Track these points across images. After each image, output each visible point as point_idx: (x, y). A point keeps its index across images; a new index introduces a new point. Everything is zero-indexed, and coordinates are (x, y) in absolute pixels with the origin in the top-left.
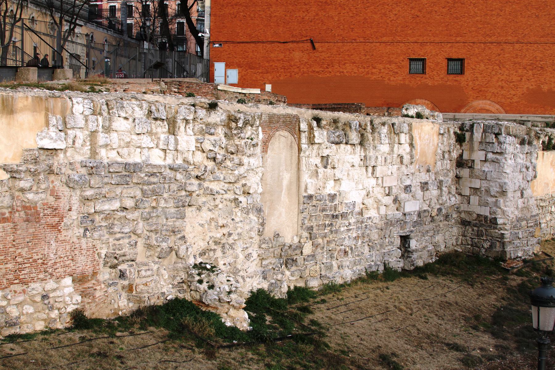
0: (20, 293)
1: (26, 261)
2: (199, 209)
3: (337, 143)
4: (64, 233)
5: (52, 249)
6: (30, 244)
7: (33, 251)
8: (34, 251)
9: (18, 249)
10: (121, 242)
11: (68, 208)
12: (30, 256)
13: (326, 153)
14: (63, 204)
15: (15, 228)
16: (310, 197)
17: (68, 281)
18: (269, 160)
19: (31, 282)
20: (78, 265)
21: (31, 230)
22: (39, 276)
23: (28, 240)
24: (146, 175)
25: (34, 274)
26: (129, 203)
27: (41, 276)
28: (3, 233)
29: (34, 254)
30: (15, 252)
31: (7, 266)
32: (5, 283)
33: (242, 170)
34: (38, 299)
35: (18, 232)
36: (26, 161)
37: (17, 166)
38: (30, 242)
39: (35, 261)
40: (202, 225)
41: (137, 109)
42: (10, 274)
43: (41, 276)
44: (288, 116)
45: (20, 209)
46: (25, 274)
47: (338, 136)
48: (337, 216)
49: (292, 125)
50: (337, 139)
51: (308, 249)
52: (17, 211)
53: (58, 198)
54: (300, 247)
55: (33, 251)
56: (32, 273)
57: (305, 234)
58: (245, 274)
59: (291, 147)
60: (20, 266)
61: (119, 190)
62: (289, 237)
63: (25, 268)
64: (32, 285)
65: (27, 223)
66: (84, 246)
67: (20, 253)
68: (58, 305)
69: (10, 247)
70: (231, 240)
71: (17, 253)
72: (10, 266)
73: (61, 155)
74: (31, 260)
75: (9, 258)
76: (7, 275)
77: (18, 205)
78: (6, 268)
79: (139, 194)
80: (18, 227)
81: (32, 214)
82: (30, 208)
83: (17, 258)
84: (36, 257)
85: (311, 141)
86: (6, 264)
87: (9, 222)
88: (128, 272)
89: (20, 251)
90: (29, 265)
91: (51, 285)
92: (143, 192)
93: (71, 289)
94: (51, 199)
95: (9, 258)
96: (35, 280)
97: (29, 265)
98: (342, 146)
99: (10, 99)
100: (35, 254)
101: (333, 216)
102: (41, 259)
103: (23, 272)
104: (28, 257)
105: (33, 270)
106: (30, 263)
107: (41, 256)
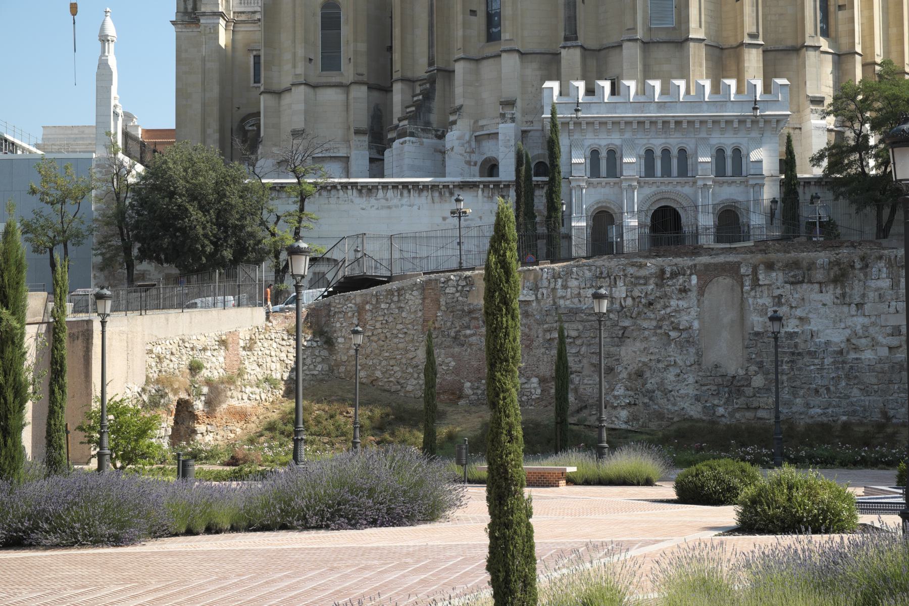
2: (635, 339)
3: (792, 283)
4: (534, 351)
13: (777, 292)
14: (533, 333)
16: (757, 334)
17: (535, 380)
18: (706, 302)
33: (668, 310)
40: (634, 352)
41: (587, 272)
44: (728, 263)
47: (794, 276)
48: (799, 354)
49: (732, 270)
50: (793, 280)
51: (758, 381)
54: (748, 379)
57: (753, 368)
58: (676, 394)
59: (732, 290)
62: (733, 367)
70: (660, 365)
73: (534, 304)
79: (581, 327)
85: (756, 283)
92: (584, 327)
98: (805, 286)
101: (793, 354)
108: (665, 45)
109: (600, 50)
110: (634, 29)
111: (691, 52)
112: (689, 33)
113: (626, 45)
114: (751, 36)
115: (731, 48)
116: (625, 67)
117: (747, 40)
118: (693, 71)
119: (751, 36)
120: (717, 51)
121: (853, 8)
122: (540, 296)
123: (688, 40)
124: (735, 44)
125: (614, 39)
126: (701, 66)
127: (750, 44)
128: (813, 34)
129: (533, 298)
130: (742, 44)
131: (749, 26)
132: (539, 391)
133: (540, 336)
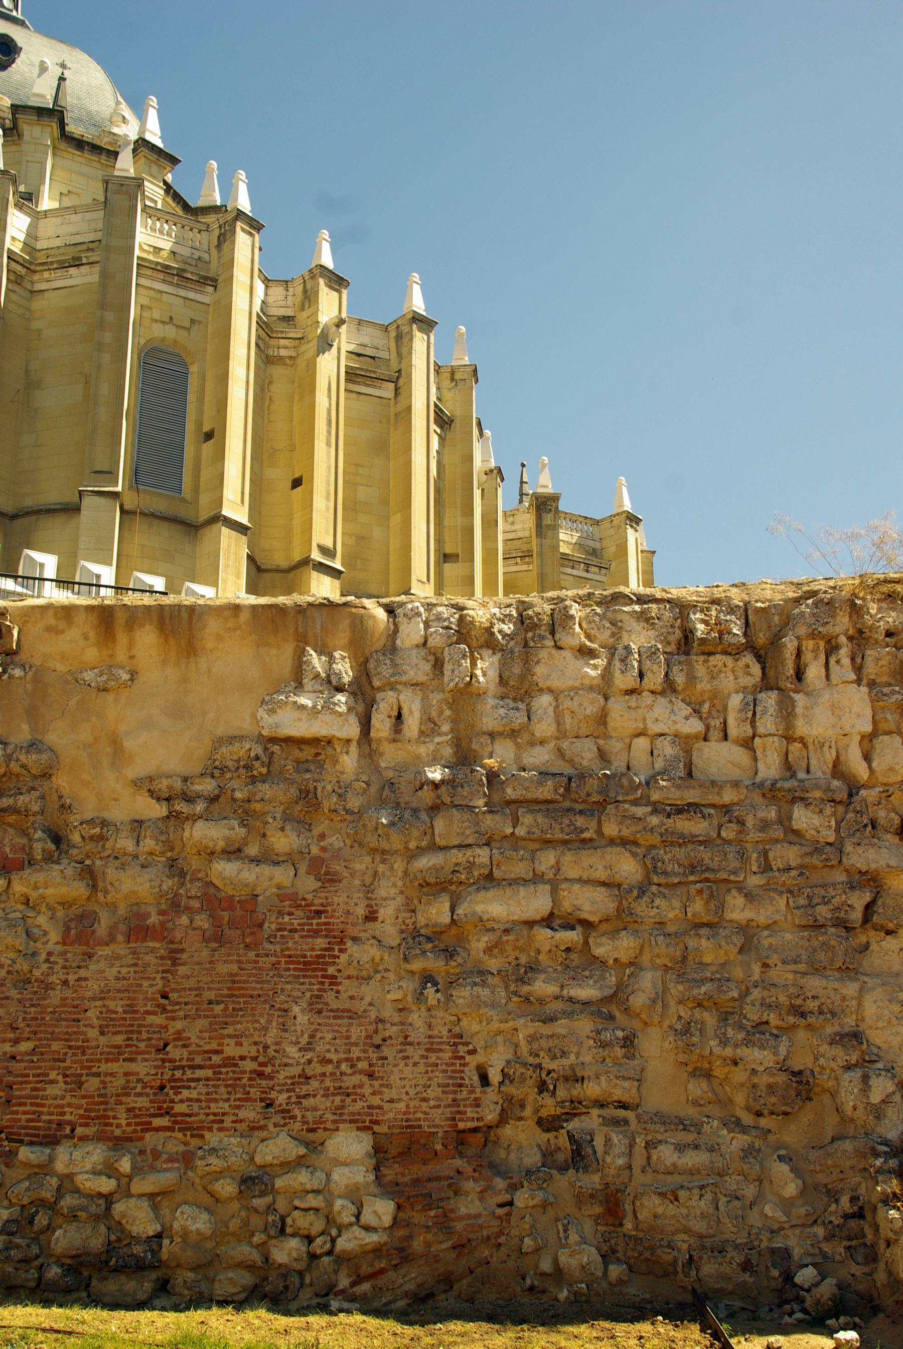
0: (171, 1160)
1: (198, 1060)
4: (347, 988)
5: (294, 1034)
6: (218, 1009)
7: (225, 1032)
8: (230, 1030)
9: (173, 1019)
10: (560, 1027)
11: (361, 911)
12: (214, 1046)
14: (347, 901)
15: (174, 957)
17: (350, 1147)
19: (210, 1129)
20: (388, 1094)
21: (223, 969)
22: (242, 1114)
23: (212, 995)
24: (655, 811)
25: (221, 1104)
26: (591, 902)
27: (249, 1113)
28: (132, 969)
29: (226, 1041)
30: (166, 1027)
31: (132, 1067)
32: (123, 1122)
34: (227, 1188)
35: (182, 970)
36: (215, 770)
37: (185, 780)
38: (218, 1003)
39: (230, 1062)
42: (139, 1095)
43: (249, 1113)
45: (196, 904)
46: (189, 1100)
52: (187, 908)
53: (329, 879)
55: (225, 1032)
56: (216, 1100)
60: (178, 1074)
61: (547, 860)
63: (198, 1080)
64: (213, 1138)
65: (214, 945)
66: (419, 1032)
67: (179, 1032)
68: (300, 1220)
69: (148, 1013)
71: (171, 1031)
72: (142, 1068)
74: (216, 1059)
75: (142, 1045)
76: (128, 1095)
77: (193, 893)
78: (126, 1074)
80: (185, 956)
81: (236, 919)
82: (229, 903)
83: (168, 1048)
84: (231, 1050)
86: (131, 1060)
87: (155, 939)
88: (599, 1142)
89: (179, 1025)
90: (209, 1073)
91: (278, 1147)
92: (652, 868)
93: (361, 1175)
94: (307, 885)
95: (142, 1045)
96: (227, 1124)
97: (209, 1073)
99: (185, 615)
100: (232, 1042)
102: (254, 1059)
103: (185, 1093)
104: (207, 1047)
105: (222, 1090)
106: (211, 1067)
107: (254, 1049)
108: (165, 525)
109: (14, 517)
110: (110, 474)
111: (223, 545)
112: (221, 506)
113: (87, 501)
114: (323, 550)
115: (278, 570)
116: (82, 545)
117: (316, 556)
118: (225, 581)
119: (323, 550)
120: (254, 570)
121: (472, 560)
122: (381, 725)
123: (218, 519)
124: (284, 564)
125: (54, 493)
126: (238, 576)
127: (321, 564)
128: (425, 580)
129: (353, 730)
130: (306, 562)
131: (323, 532)
132: (381, 1210)
133: (386, 912)
